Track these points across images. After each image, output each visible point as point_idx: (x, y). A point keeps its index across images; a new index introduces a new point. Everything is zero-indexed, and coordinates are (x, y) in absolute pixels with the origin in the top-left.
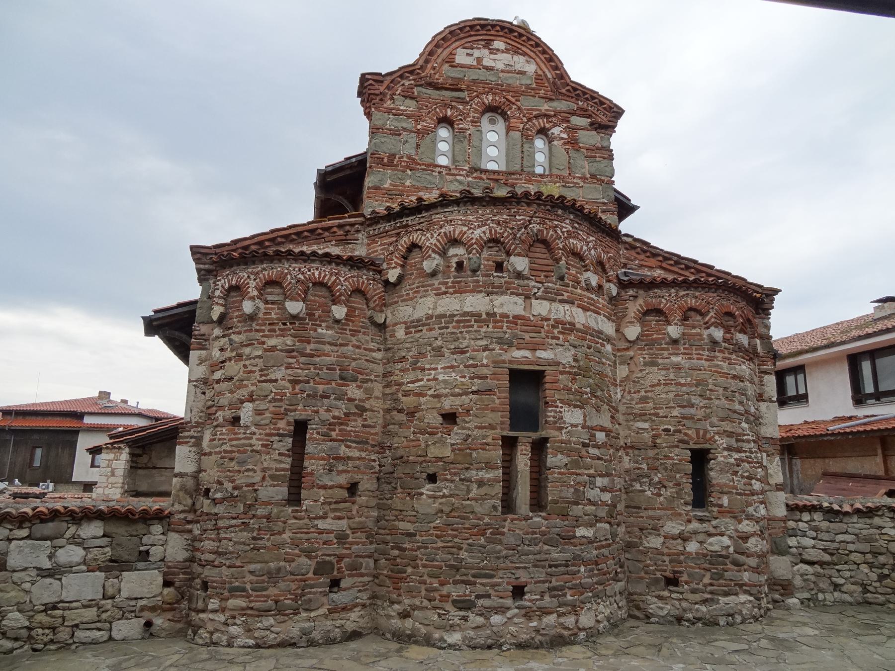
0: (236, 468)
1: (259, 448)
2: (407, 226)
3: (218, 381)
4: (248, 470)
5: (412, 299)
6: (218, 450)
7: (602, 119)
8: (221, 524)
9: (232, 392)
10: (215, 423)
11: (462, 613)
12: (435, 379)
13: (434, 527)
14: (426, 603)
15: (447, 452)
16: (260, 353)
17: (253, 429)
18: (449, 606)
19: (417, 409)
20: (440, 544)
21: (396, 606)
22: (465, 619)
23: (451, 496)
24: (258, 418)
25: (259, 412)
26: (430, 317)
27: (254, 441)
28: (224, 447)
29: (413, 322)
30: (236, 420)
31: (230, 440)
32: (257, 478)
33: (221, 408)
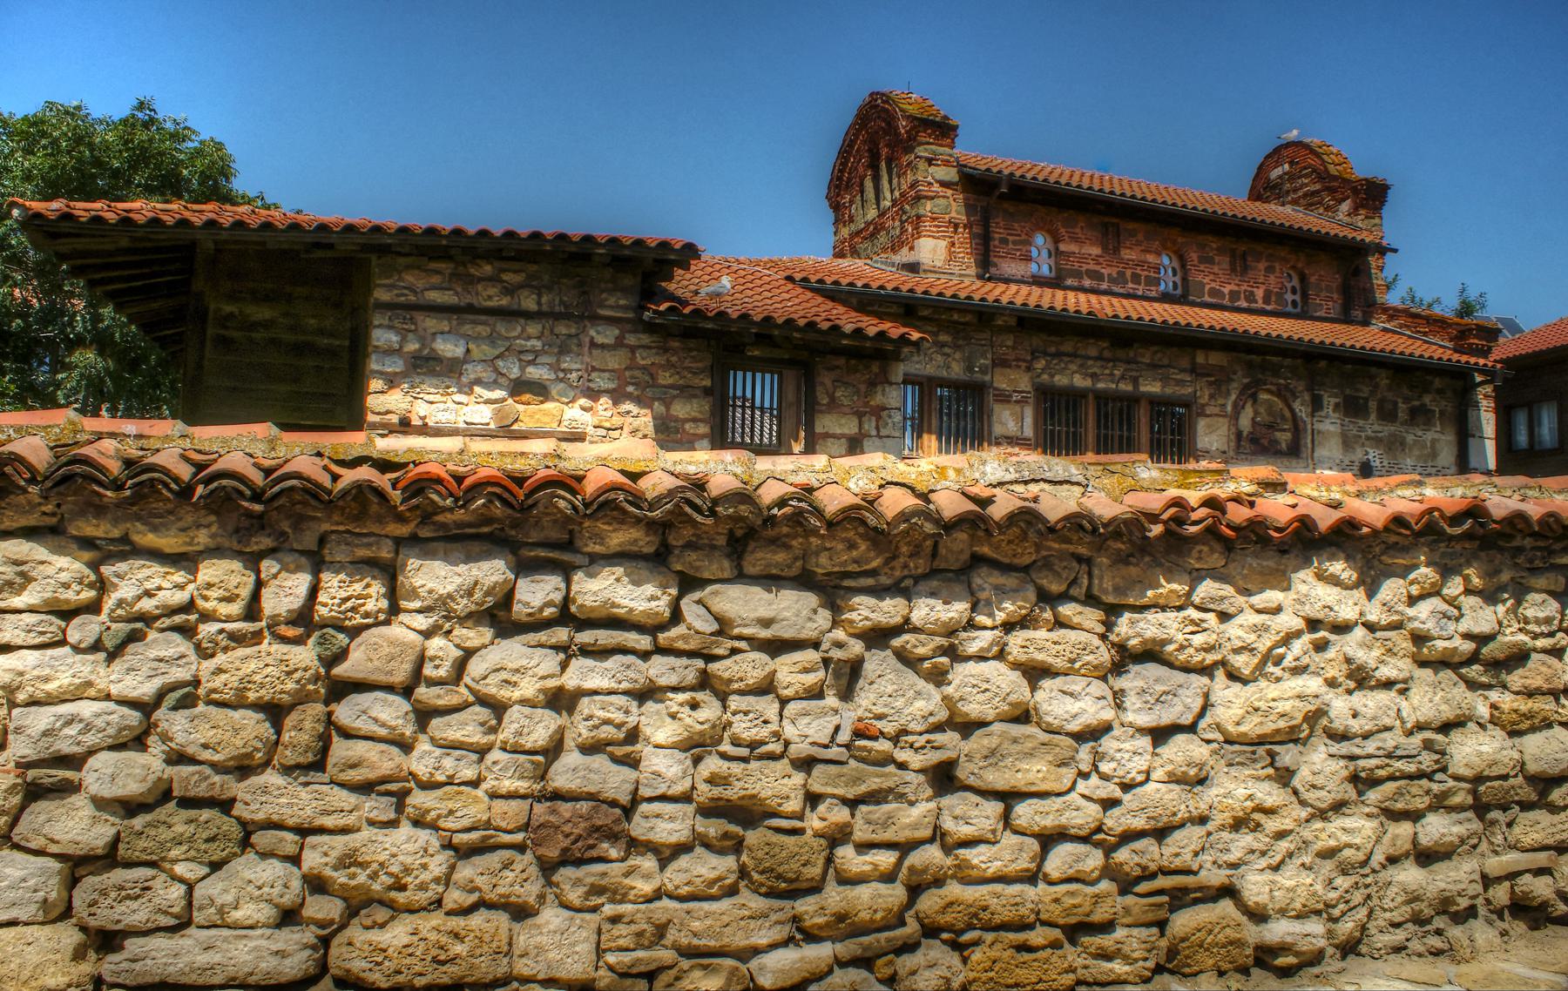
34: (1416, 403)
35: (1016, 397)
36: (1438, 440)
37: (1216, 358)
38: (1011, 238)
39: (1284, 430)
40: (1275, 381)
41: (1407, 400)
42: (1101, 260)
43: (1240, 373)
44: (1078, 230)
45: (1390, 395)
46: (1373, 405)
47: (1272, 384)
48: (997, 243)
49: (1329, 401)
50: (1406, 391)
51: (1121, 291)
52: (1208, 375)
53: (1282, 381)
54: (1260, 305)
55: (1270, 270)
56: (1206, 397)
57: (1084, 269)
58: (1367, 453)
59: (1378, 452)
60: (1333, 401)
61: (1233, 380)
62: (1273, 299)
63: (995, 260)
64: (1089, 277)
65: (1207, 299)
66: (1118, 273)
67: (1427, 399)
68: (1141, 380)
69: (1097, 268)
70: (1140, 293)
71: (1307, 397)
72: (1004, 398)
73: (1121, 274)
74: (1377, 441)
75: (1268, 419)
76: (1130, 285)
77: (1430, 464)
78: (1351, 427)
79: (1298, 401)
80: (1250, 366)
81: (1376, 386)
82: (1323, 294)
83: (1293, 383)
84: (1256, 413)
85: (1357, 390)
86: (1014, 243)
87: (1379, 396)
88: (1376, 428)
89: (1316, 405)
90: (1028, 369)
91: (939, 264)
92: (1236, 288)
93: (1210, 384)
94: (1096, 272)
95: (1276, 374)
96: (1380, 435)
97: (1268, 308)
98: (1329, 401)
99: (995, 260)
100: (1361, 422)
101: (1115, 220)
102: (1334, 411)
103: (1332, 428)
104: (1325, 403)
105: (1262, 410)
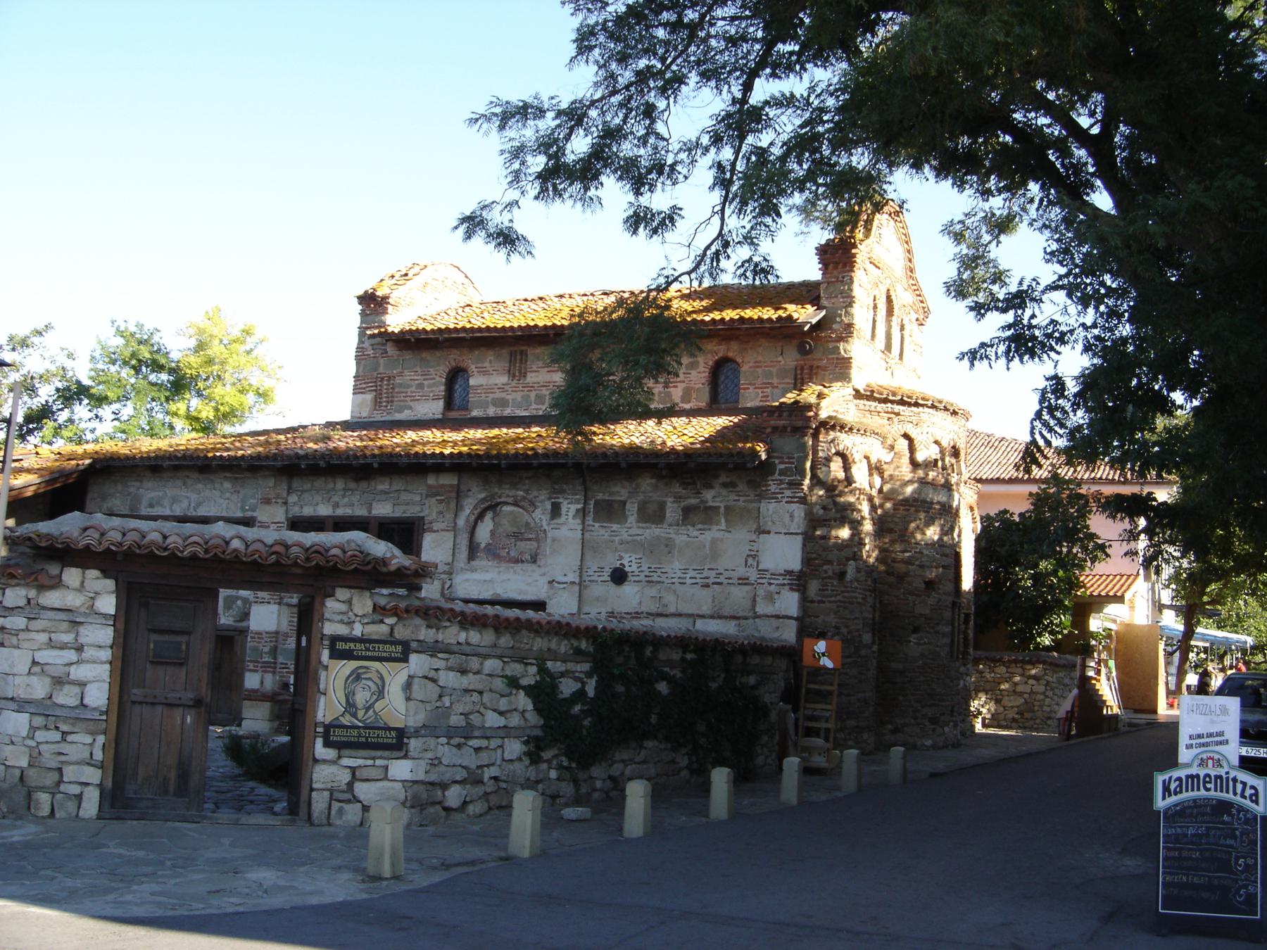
0: (849, 616)
1: (860, 600)
2: (898, 414)
4: (856, 618)
6: (833, 599)
7: (921, 317)
11: (933, 727)
12: (921, 553)
13: (919, 667)
14: (913, 721)
15: (927, 612)
17: (856, 584)
18: (927, 723)
19: (907, 574)
20: (922, 678)
21: (890, 726)
22: (934, 730)
23: (929, 643)
24: (859, 575)
27: (857, 595)
28: (839, 598)
30: (842, 575)
31: (843, 592)
32: (861, 627)
33: (830, 562)
34: (693, 501)
36: (722, 540)
37: (449, 480)
38: (426, 382)
39: (529, 539)
40: (512, 493)
41: (678, 498)
42: (507, 387)
43: (475, 489)
44: (487, 365)
45: (656, 497)
46: (632, 508)
47: (508, 496)
48: (413, 389)
49: (570, 508)
50: (677, 489)
51: (526, 414)
52: (438, 494)
53: (521, 493)
55: (692, 366)
56: (434, 515)
57: (489, 399)
58: (621, 558)
59: (634, 556)
60: (574, 507)
61: (467, 496)
62: (694, 396)
63: (411, 404)
64: (494, 405)
66: (523, 397)
67: (708, 495)
68: (374, 504)
69: (503, 395)
71: (548, 506)
73: (526, 398)
74: (633, 545)
75: (510, 529)
76: (534, 406)
77: (706, 568)
78: (602, 531)
79: (538, 511)
81: (638, 486)
82: (759, 381)
84: (496, 525)
85: (611, 494)
86: (429, 386)
87: (641, 497)
88: (639, 531)
89: (556, 511)
90: (286, 503)
91: (364, 415)
93: (440, 502)
94: (503, 399)
95: (514, 486)
96: (639, 538)
97: (687, 406)
98: (570, 508)
99: (411, 404)
100: (615, 527)
101: (524, 348)
102: (574, 517)
103: (570, 534)
104: (564, 510)
105: (505, 521)
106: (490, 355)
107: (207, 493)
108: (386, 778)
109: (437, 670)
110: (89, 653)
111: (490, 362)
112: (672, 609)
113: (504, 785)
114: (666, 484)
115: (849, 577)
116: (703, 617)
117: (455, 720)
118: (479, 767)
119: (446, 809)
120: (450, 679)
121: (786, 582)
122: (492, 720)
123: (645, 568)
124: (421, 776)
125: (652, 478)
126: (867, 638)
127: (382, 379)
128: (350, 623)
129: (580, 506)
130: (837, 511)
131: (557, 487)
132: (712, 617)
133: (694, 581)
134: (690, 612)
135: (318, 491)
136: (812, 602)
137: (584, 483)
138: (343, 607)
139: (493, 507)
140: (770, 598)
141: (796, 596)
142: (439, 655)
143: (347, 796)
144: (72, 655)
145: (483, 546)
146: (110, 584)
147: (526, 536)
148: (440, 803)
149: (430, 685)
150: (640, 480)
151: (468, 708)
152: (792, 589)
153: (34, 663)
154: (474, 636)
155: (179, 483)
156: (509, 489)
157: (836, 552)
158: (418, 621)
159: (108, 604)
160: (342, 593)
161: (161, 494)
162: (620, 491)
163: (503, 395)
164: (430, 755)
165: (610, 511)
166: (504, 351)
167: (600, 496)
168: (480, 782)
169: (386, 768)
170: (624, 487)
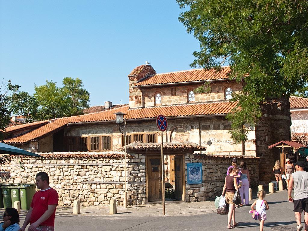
3: (260, 131)
5: (275, 115)
8: (266, 160)
9: (264, 134)
10: (261, 140)
16: (268, 126)
17: (268, 142)
25: (268, 138)
26: (279, 119)
28: (265, 145)
29: (275, 120)
30: (265, 140)
33: (262, 137)
34: (227, 124)
35: (117, 137)
39: (186, 136)
41: (223, 123)
43: (171, 124)
45: (218, 123)
46: (211, 126)
50: (223, 121)
54: (216, 99)
57: (167, 101)
58: (210, 139)
59: (213, 138)
62: (220, 97)
65: (200, 101)
68: (144, 130)
69: (170, 99)
70: (181, 103)
72: (115, 137)
80: (173, 122)
81: (213, 121)
83: (186, 124)
85: (206, 123)
87: (214, 124)
92: (209, 96)
97: (219, 100)
101: (175, 87)
106: (166, 89)
107: (98, 129)
108: (199, 192)
109: (206, 168)
110: (141, 171)
111: (166, 91)
112: (224, 151)
113: (217, 192)
114: (220, 120)
115: (266, 140)
116: (232, 152)
117: (210, 179)
118: (213, 188)
119: (210, 197)
120: (208, 170)
121: (252, 142)
122: (215, 178)
123: (216, 141)
124: (206, 191)
125: (216, 119)
126: (272, 155)
127: (137, 97)
128: (190, 161)
129: (198, 127)
130: (263, 124)
131: (192, 122)
132: (234, 152)
133: (229, 143)
134: (229, 151)
135: (129, 127)
136: (259, 146)
137: (199, 121)
138: (188, 157)
139: (175, 129)
140: (249, 146)
141: (255, 145)
142: (206, 166)
143: (192, 196)
144: (138, 172)
145: (173, 138)
146: (144, 156)
147: (185, 135)
148: (208, 196)
149: (206, 172)
150: (213, 120)
151: (211, 176)
152: (254, 144)
153: (131, 174)
154: (211, 161)
155: (90, 127)
156: (180, 124)
157: (263, 134)
158: (203, 159)
159: (144, 161)
160: (188, 155)
161: (85, 130)
162: (208, 123)
163: (170, 99)
164: (206, 186)
165: (206, 128)
166: (169, 88)
167: (203, 124)
168: (214, 191)
169: (199, 189)
170: (209, 122)
